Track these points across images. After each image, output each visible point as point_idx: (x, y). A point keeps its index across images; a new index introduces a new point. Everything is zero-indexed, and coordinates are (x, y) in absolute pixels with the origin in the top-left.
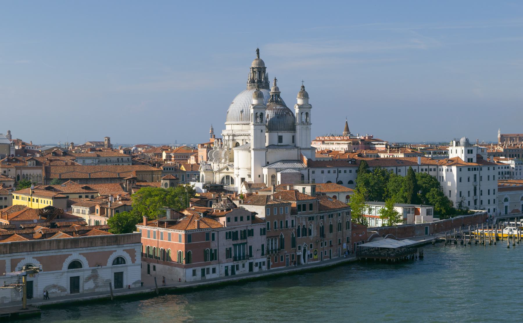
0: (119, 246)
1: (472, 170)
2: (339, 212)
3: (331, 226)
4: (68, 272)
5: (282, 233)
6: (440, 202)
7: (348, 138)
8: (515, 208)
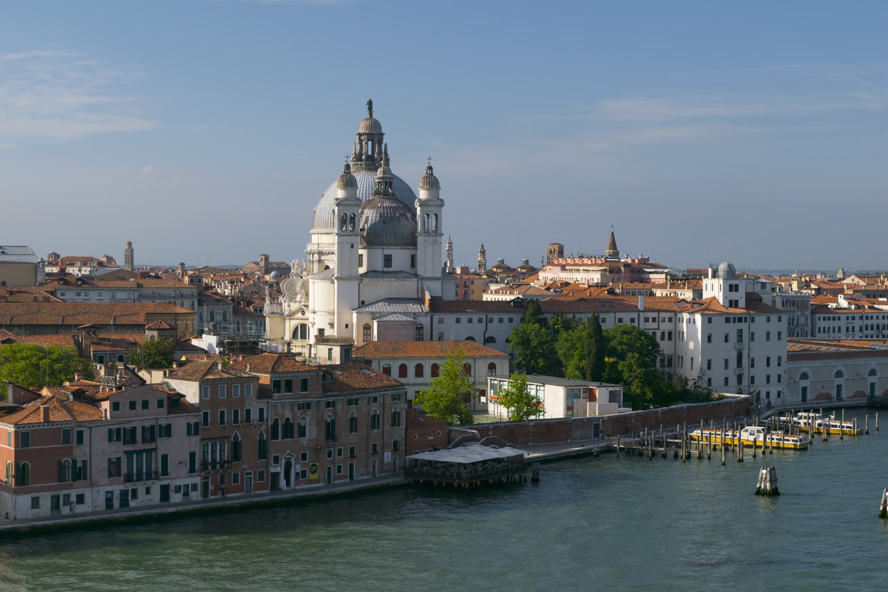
1: (734, 322)
2: (373, 395)
5: (236, 431)
6: (641, 378)
7: (603, 262)
8: (823, 392)
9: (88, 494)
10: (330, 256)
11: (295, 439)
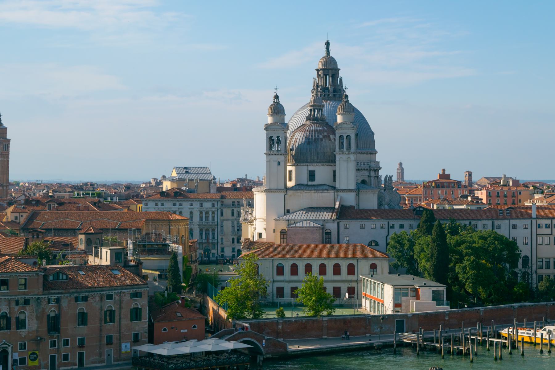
6: (472, 279)
11: (12, 330)
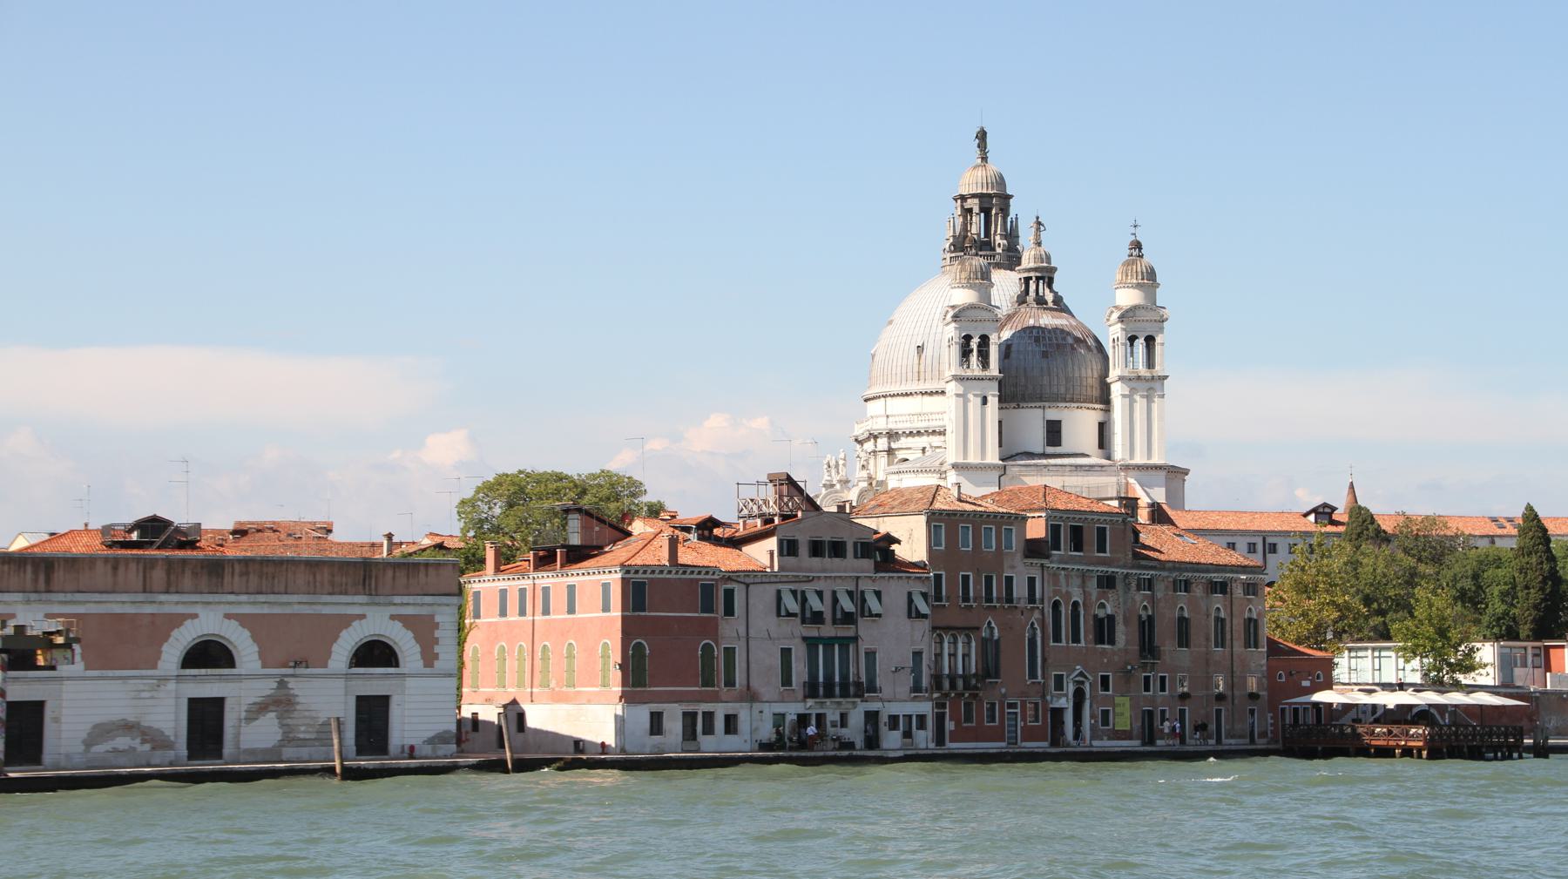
0: (377, 599)
3: (1183, 623)
4: (179, 678)
5: (990, 619)
9: (744, 713)
10: (910, 439)
